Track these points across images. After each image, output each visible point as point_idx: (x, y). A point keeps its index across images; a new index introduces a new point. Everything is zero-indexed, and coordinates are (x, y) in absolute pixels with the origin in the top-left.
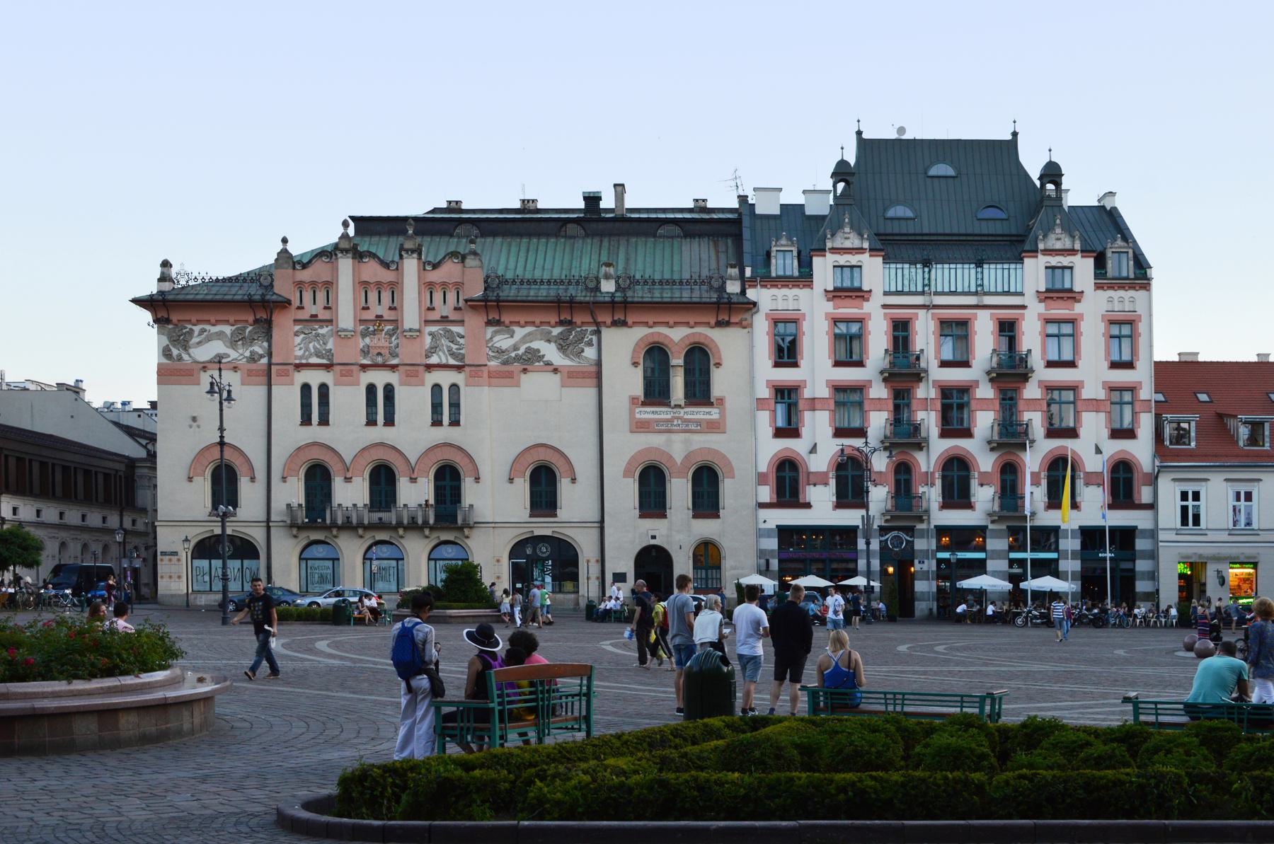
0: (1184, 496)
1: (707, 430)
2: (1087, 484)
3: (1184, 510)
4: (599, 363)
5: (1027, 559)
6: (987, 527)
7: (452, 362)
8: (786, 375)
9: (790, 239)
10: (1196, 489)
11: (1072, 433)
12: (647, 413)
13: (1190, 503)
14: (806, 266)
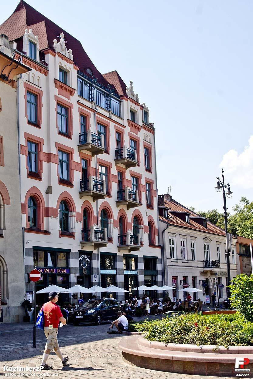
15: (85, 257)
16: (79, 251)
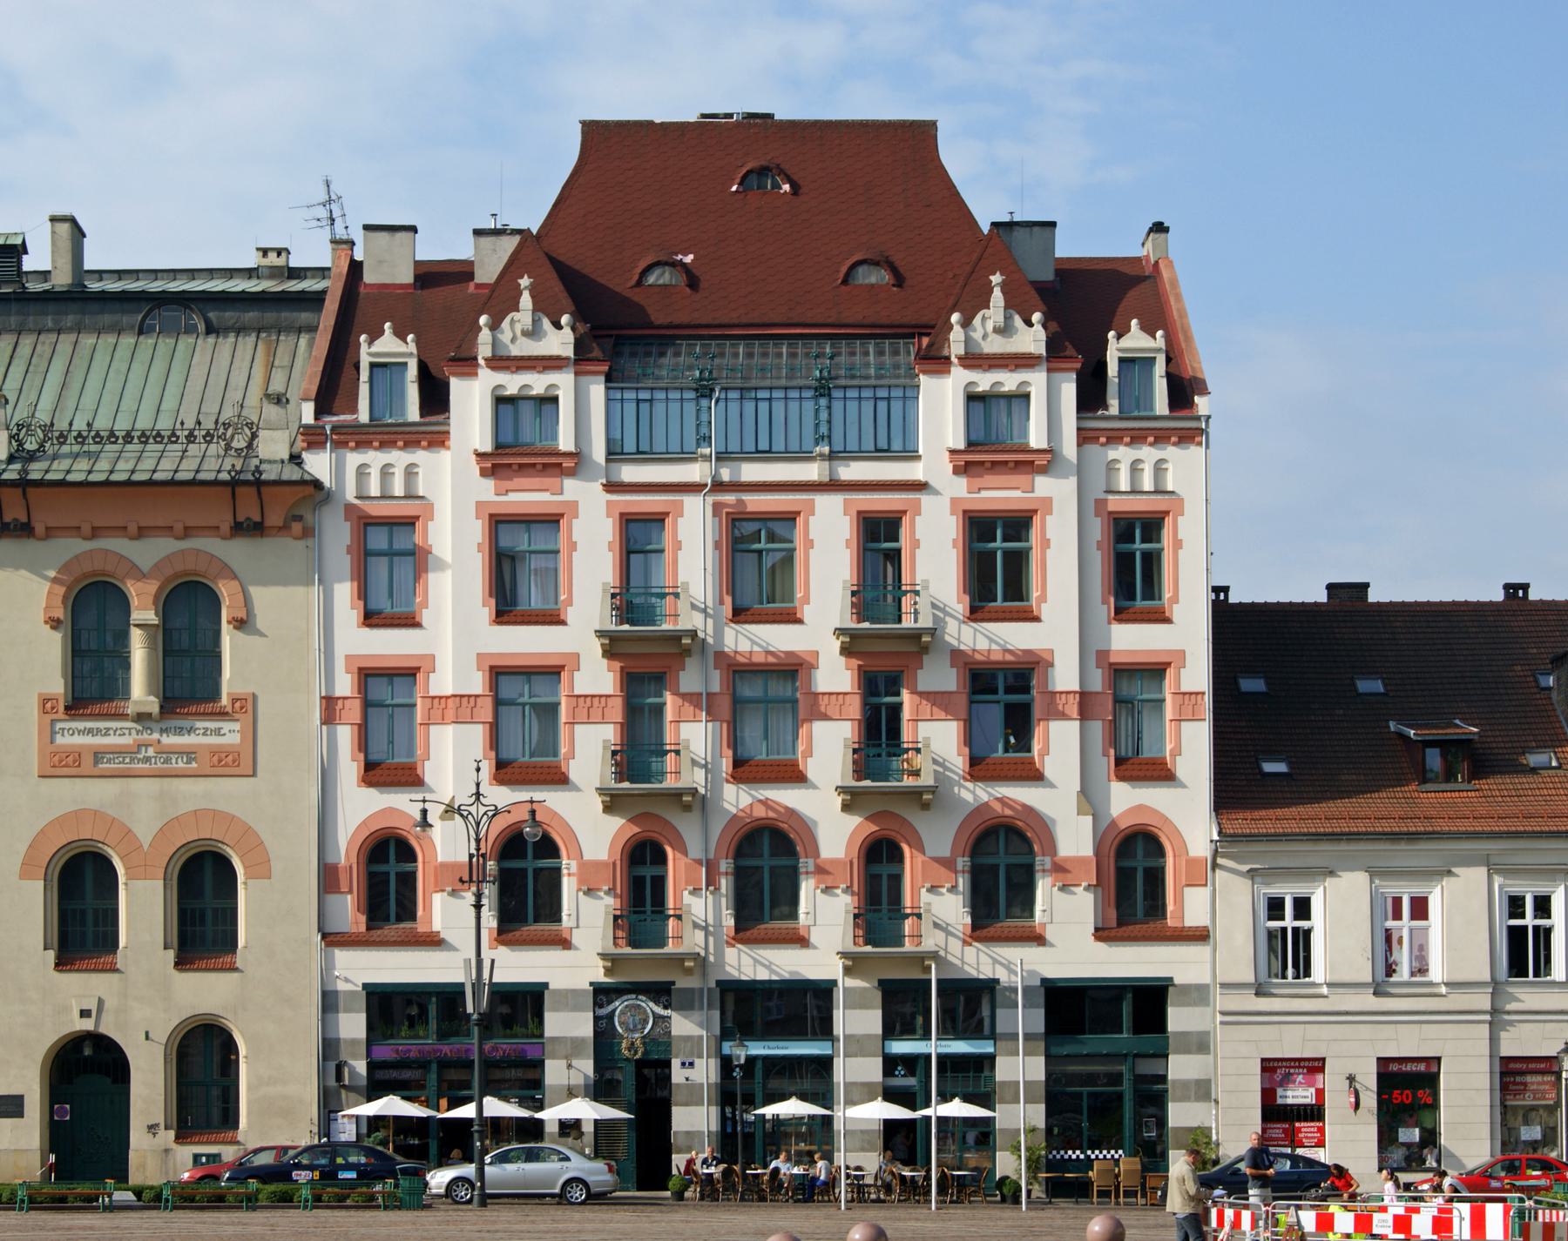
1: (209, 771)
5: (928, 1057)
6: (834, 983)
8: (389, 644)
9: (401, 335)
12: (77, 735)
14: (435, 398)
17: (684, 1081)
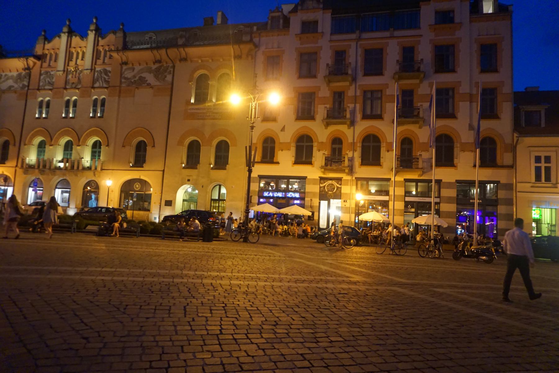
0: (538, 159)
2: (463, 151)
3: (538, 170)
4: (172, 84)
7: (105, 85)
10: (547, 154)
11: (453, 116)
13: (543, 165)
15: (334, 182)
16: (319, 177)
17: (344, 206)
